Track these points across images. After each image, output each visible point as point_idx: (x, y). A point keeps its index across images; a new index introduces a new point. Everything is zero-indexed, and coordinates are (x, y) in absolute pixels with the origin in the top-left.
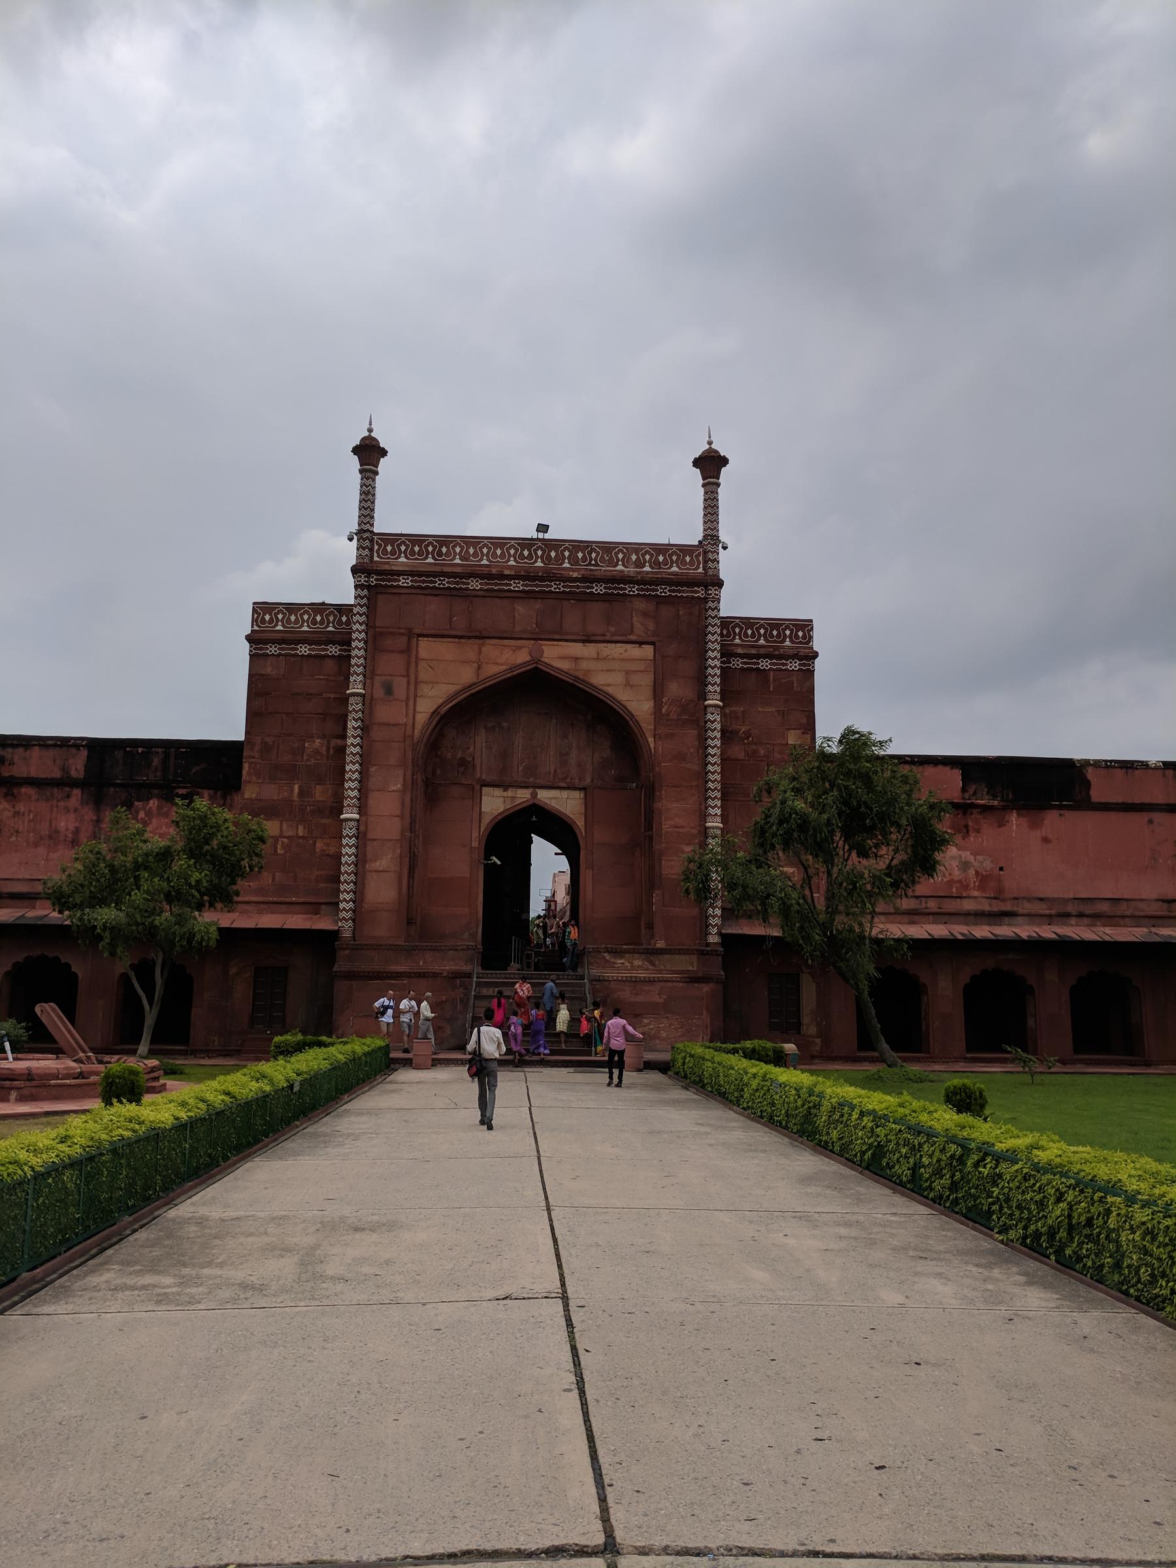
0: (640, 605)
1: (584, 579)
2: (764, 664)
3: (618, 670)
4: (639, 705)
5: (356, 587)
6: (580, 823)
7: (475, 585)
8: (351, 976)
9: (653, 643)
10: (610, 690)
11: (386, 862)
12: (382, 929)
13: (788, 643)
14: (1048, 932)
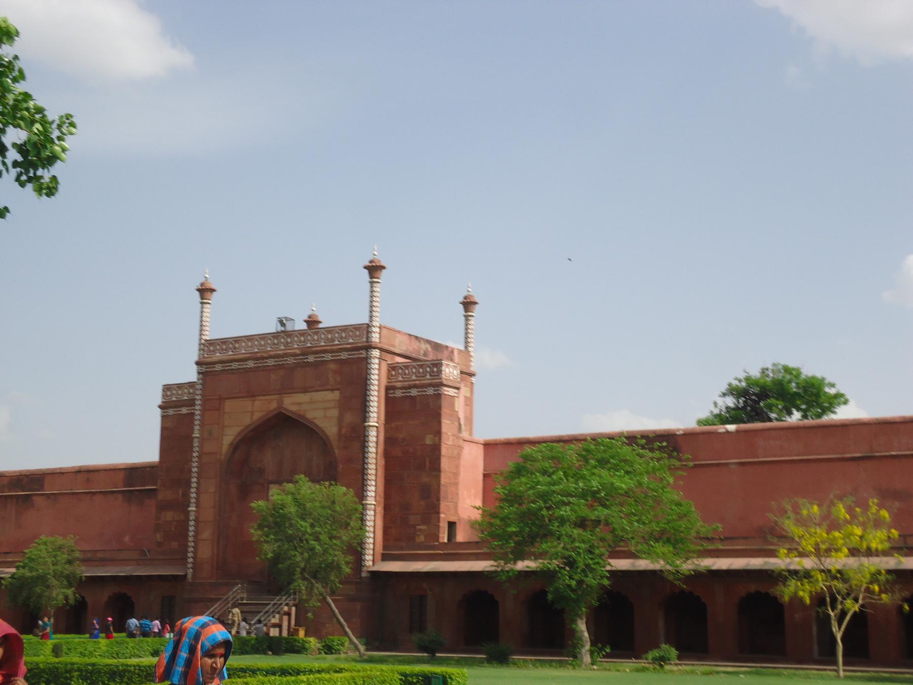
0: (332, 366)
1: (302, 354)
2: (414, 392)
4: (331, 429)
5: (199, 373)
9: (338, 389)
10: (316, 422)
13: (428, 377)
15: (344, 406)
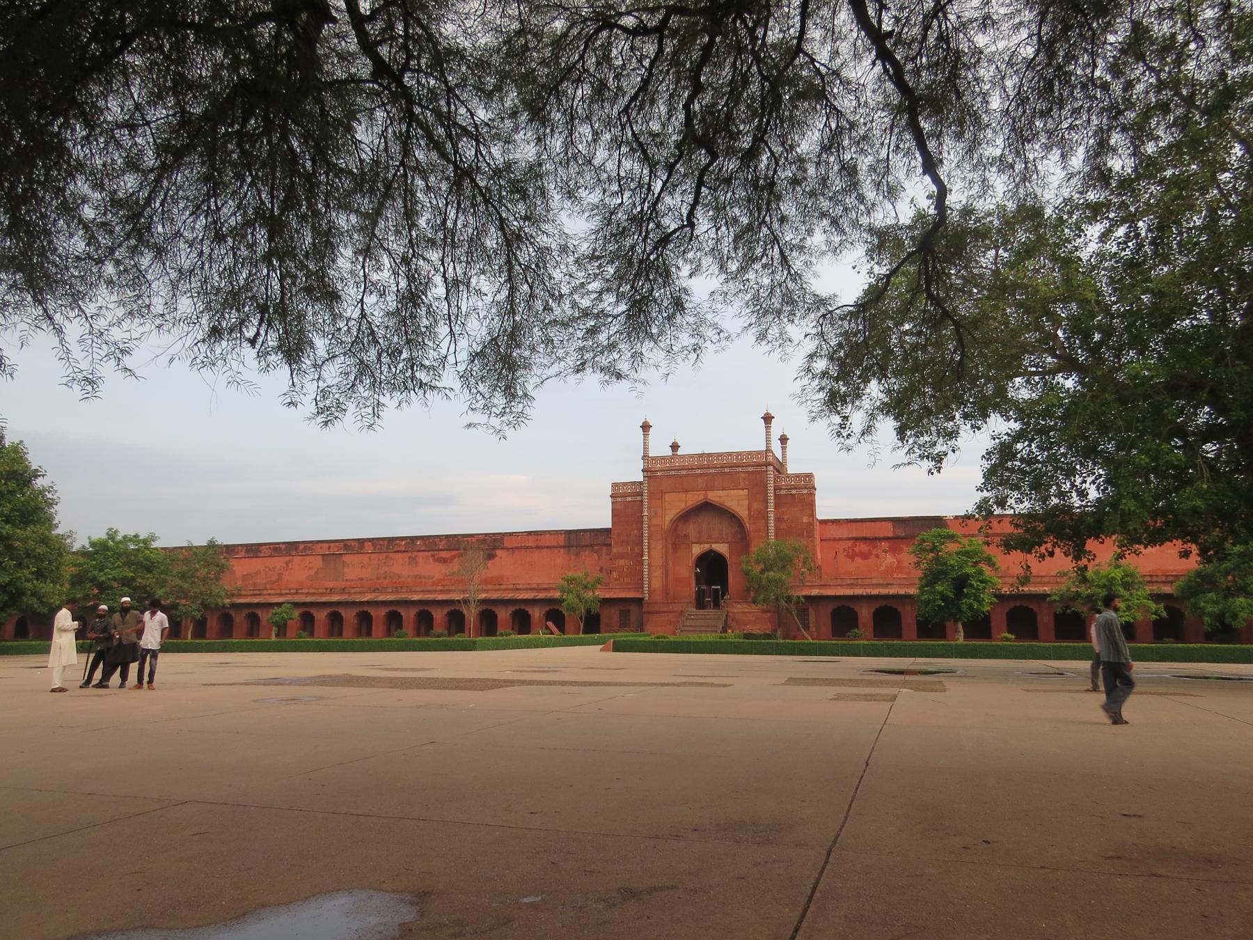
0: (742, 475)
2: (794, 492)
3: (735, 500)
4: (743, 512)
6: (727, 556)
7: (684, 472)
8: (648, 613)
11: (658, 573)
12: (658, 597)
14: (902, 592)
15: (752, 498)
